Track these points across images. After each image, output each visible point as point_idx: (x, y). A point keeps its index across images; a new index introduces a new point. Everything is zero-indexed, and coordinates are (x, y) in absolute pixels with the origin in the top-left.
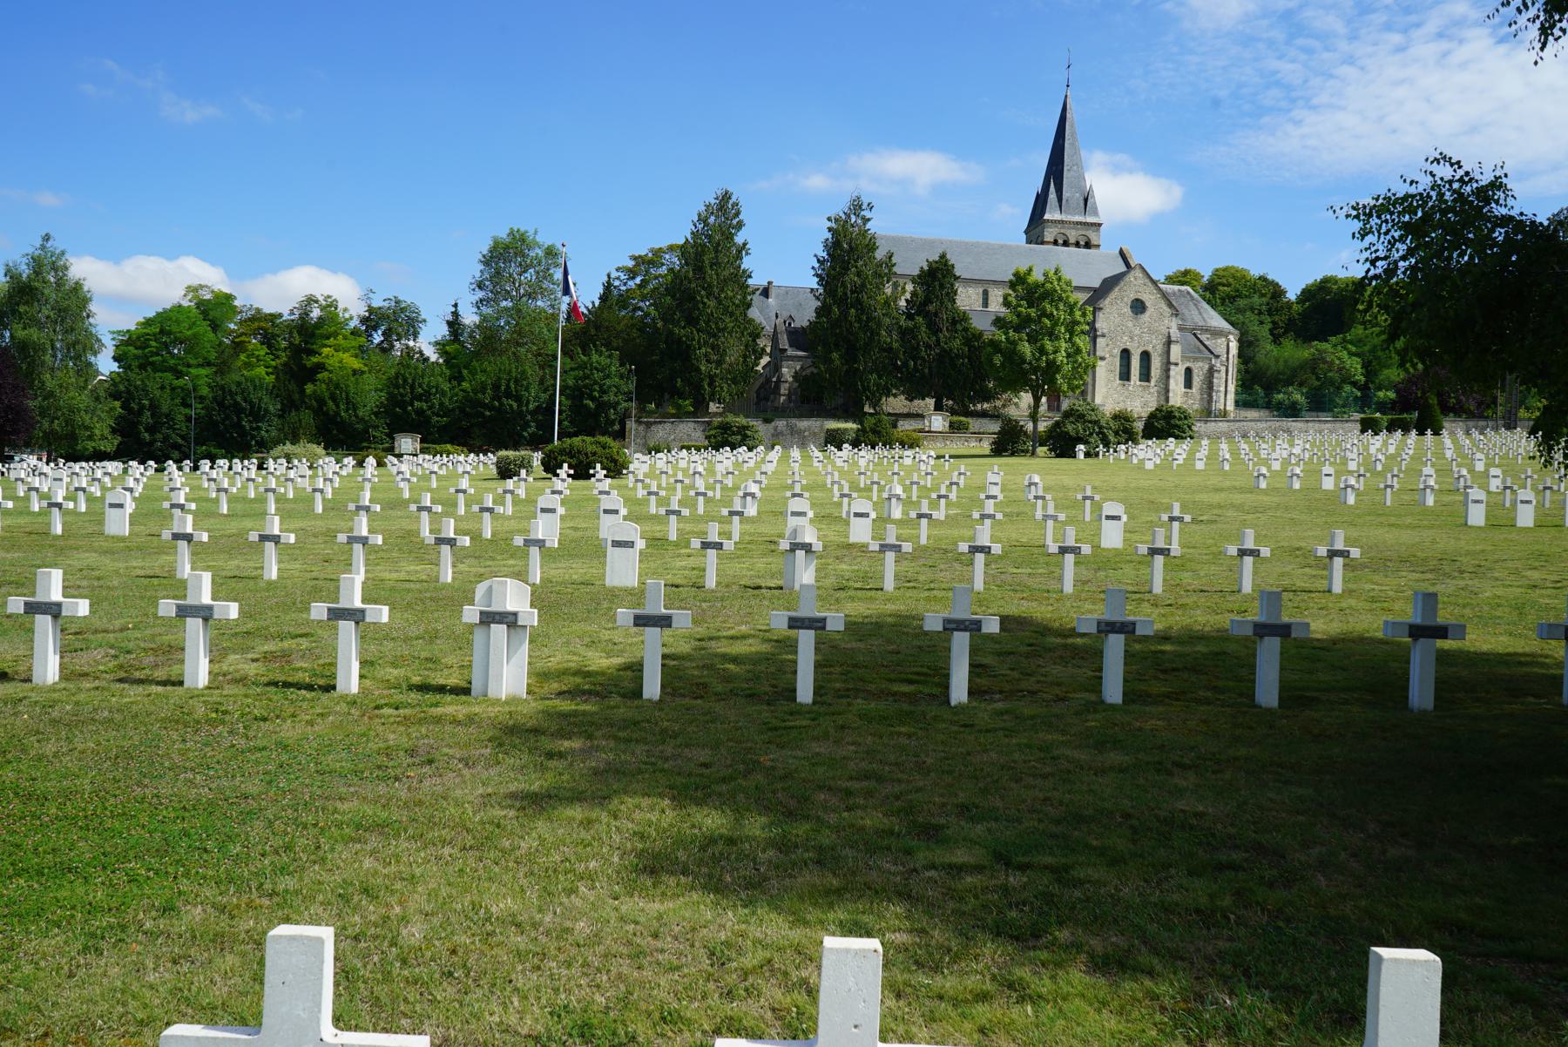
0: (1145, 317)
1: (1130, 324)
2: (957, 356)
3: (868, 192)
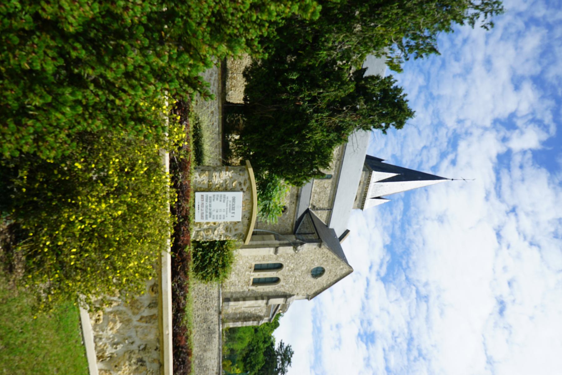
0: (309, 278)
1: (304, 268)
2: (303, 138)
3: (505, 14)
